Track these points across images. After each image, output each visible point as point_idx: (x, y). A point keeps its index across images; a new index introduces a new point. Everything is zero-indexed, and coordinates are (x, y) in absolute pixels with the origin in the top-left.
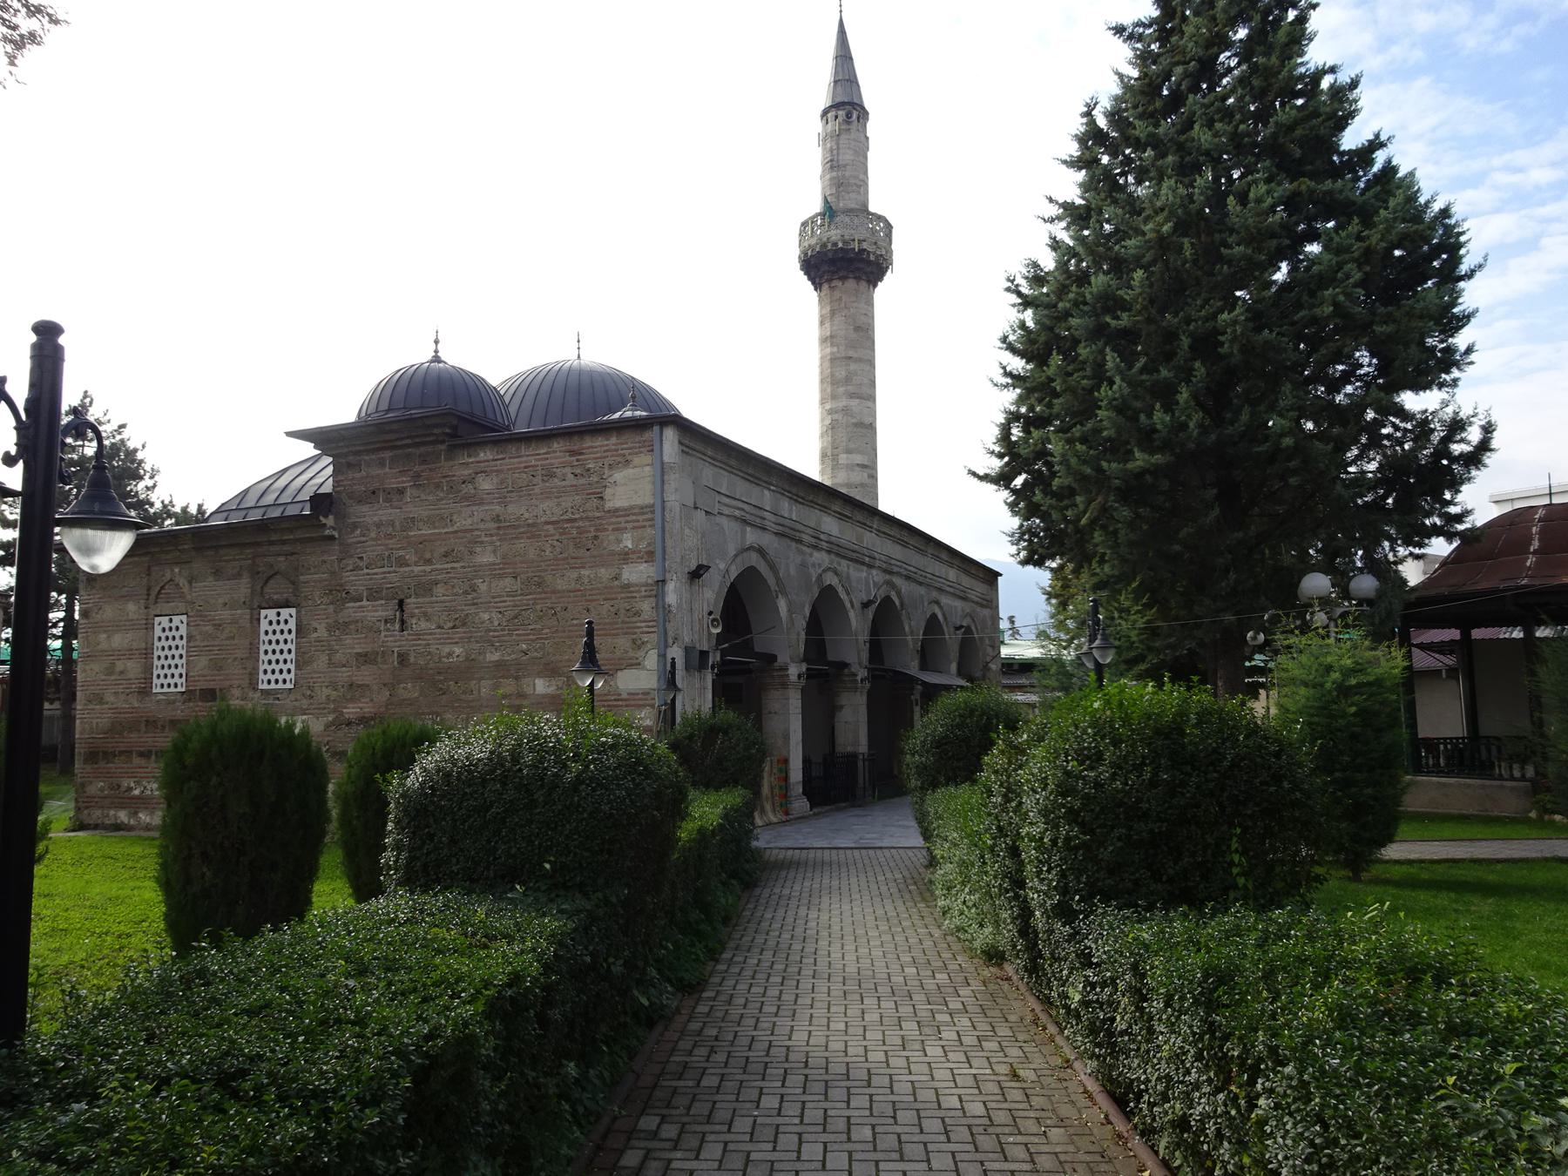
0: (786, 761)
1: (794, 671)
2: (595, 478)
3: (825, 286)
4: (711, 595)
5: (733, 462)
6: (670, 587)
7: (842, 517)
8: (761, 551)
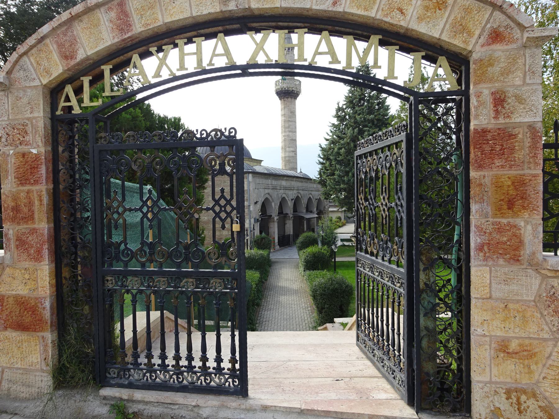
1: (276, 218)
4: (259, 206)
6: (251, 207)
8: (269, 194)
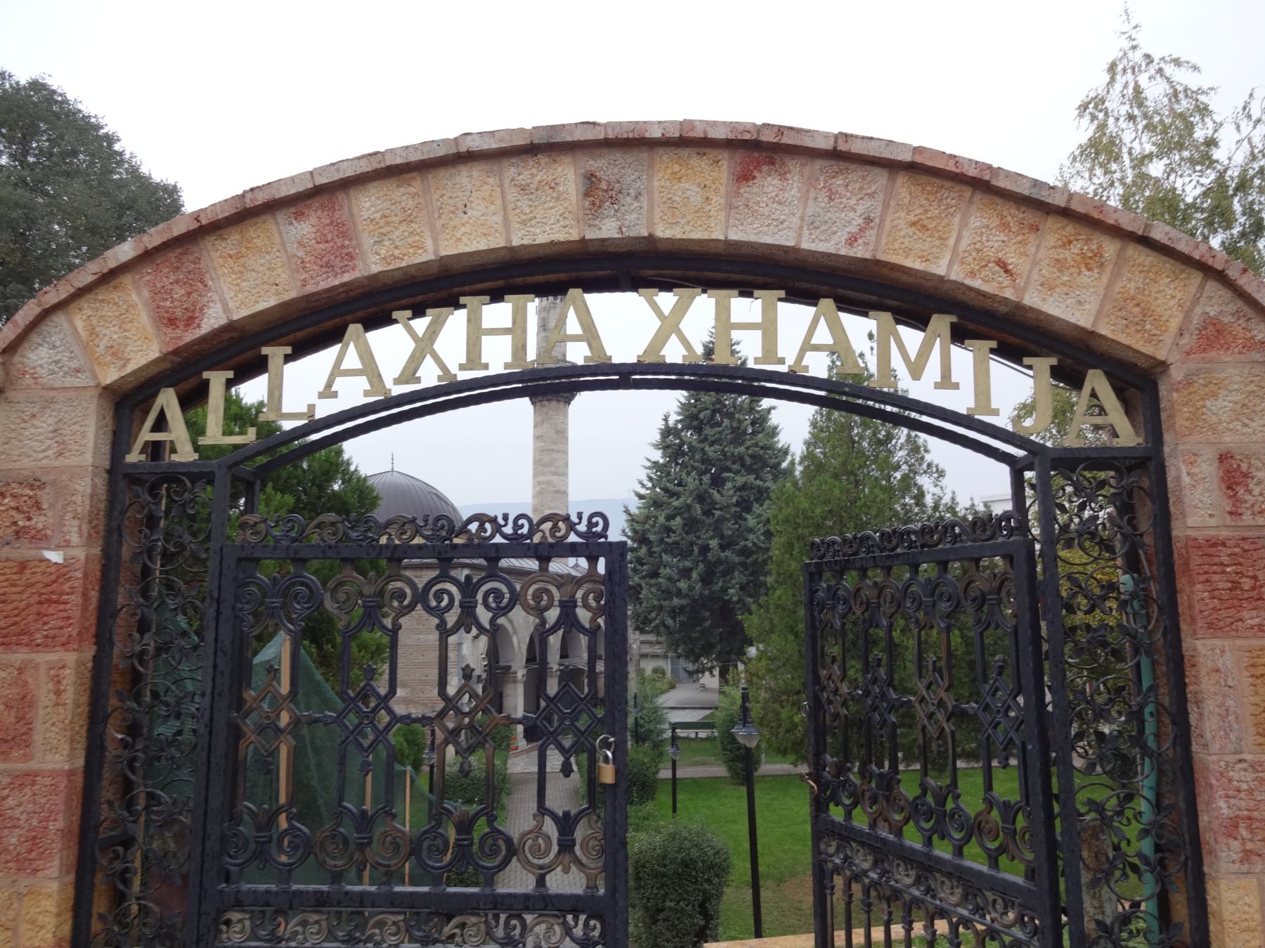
1: (521, 673)
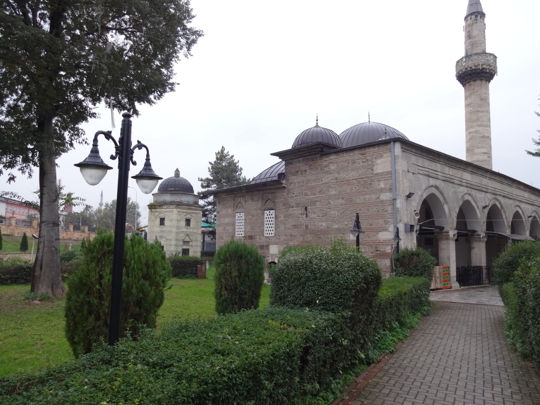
0: (449, 268)
1: (452, 233)
2: (370, 163)
3: (467, 85)
4: (416, 204)
5: (424, 154)
6: (398, 201)
7: (472, 173)
8: (437, 187)
